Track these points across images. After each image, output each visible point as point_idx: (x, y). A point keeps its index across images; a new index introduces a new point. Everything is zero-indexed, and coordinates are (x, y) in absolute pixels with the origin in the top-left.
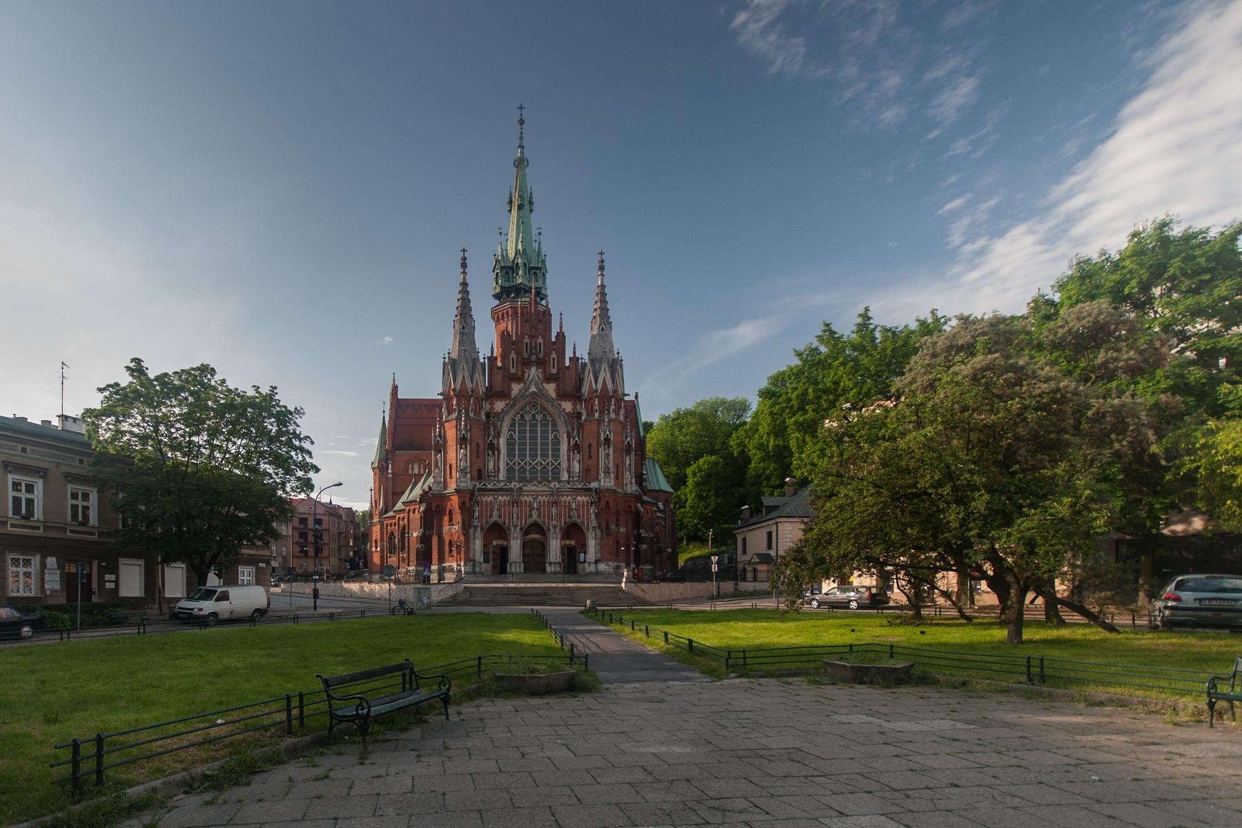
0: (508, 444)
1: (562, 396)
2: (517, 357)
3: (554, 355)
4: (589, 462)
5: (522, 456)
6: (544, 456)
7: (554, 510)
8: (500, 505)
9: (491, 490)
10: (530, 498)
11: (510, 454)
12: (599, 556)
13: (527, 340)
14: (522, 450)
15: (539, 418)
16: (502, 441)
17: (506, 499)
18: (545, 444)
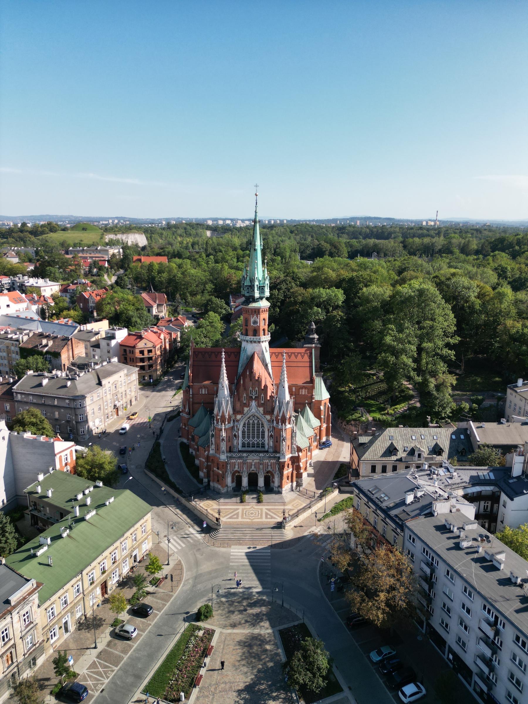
0: (243, 432)
1: (266, 413)
2: (247, 396)
3: (262, 395)
4: (277, 444)
5: (248, 438)
6: (258, 437)
7: (261, 466)
8: (238, 464)
9: (234, 457)
10: (251, 461)
11: (243, 437)
12: (279, 484)
13: (251, 389)
14: (249, 435)
15: (256, 422)
16: (240, 433)
17: (241, 461)
18: (258, 432)
